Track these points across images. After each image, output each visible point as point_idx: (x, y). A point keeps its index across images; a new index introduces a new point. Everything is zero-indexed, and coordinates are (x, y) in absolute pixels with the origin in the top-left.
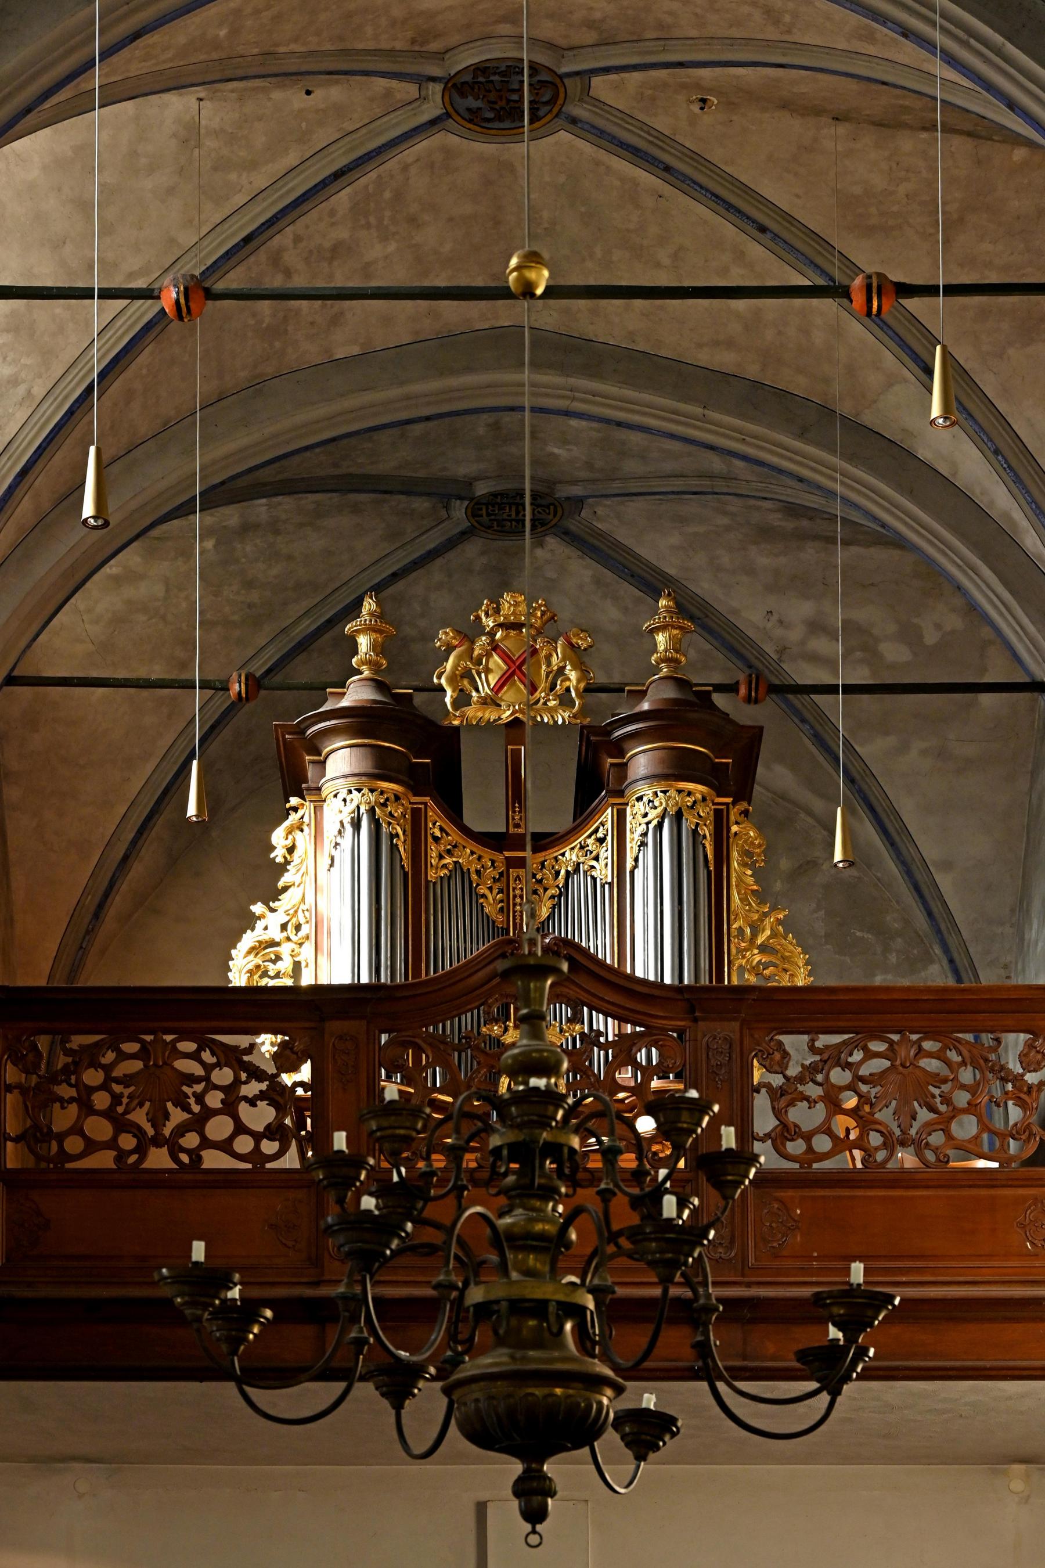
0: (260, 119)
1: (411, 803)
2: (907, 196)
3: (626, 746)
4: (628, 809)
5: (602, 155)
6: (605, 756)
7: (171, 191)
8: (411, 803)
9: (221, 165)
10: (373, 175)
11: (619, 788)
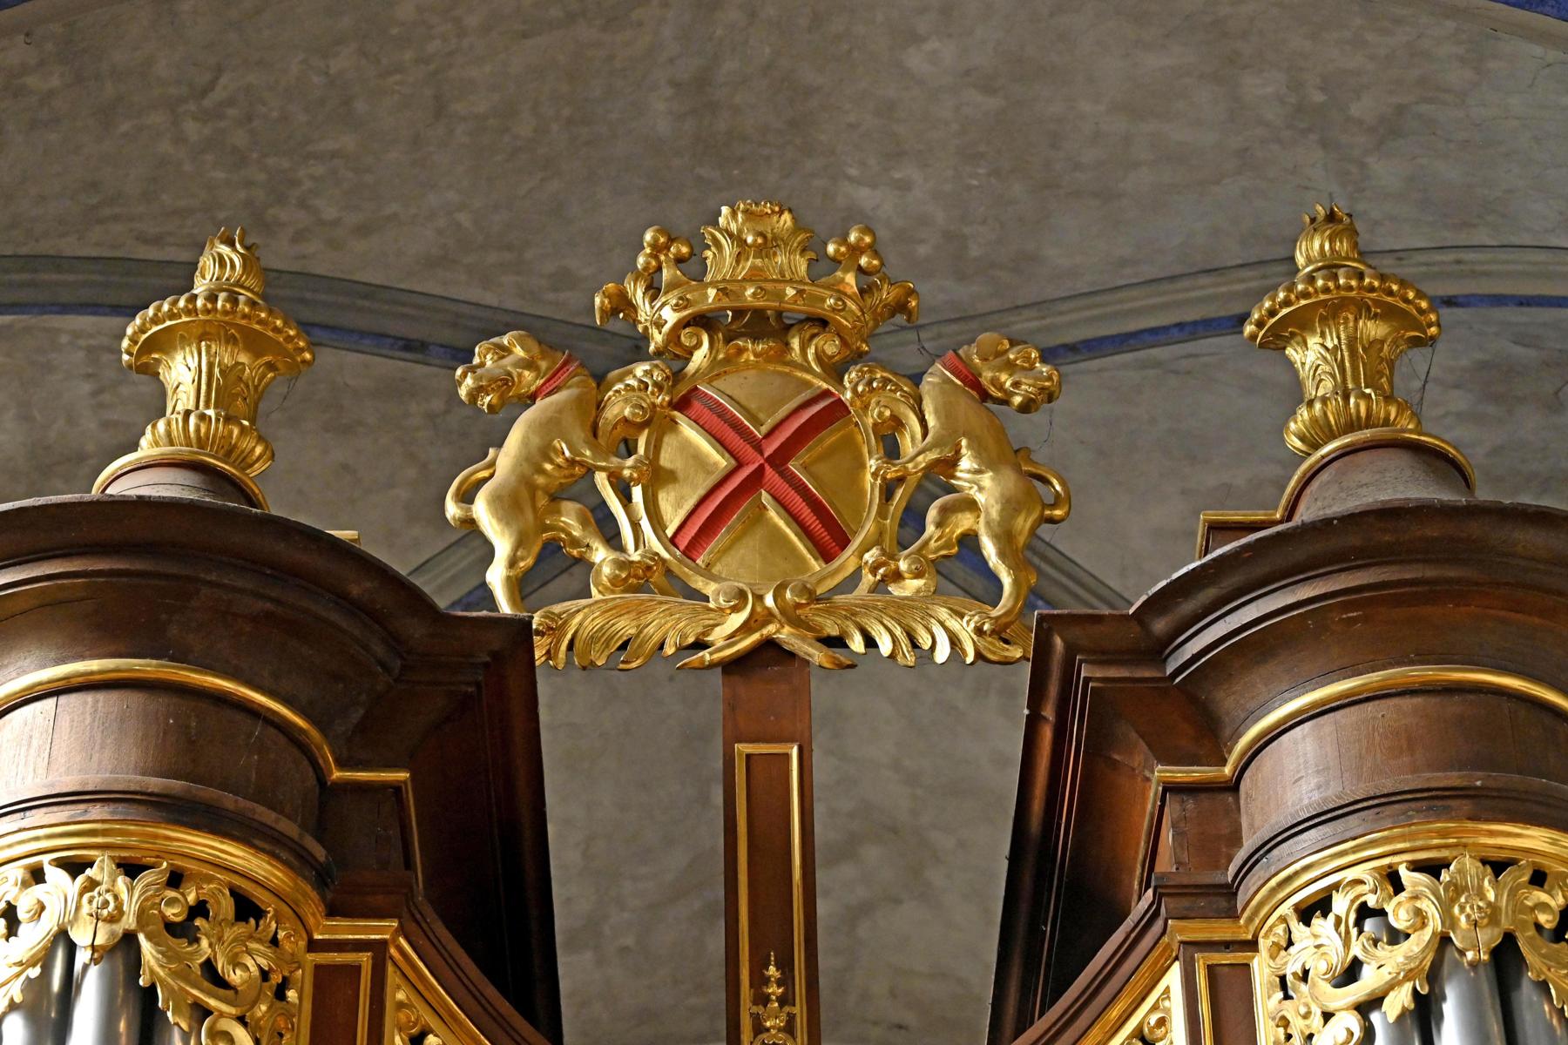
1: (313, 946)
3: (1227, 701)
4: (1262, 968)
6: (1140, 754)
8: (313, 946)
11: (1217, 878)
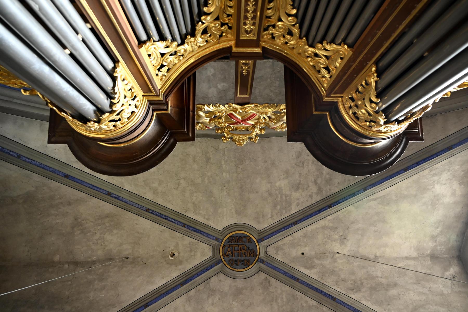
0: (319, 245)
2: (96, 233)
5: (206, 222)
7: (353, 223)
9: (334, 229)
10: (283, 217)
